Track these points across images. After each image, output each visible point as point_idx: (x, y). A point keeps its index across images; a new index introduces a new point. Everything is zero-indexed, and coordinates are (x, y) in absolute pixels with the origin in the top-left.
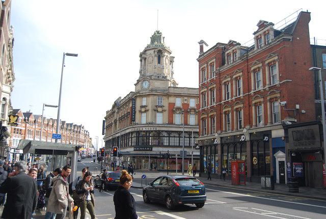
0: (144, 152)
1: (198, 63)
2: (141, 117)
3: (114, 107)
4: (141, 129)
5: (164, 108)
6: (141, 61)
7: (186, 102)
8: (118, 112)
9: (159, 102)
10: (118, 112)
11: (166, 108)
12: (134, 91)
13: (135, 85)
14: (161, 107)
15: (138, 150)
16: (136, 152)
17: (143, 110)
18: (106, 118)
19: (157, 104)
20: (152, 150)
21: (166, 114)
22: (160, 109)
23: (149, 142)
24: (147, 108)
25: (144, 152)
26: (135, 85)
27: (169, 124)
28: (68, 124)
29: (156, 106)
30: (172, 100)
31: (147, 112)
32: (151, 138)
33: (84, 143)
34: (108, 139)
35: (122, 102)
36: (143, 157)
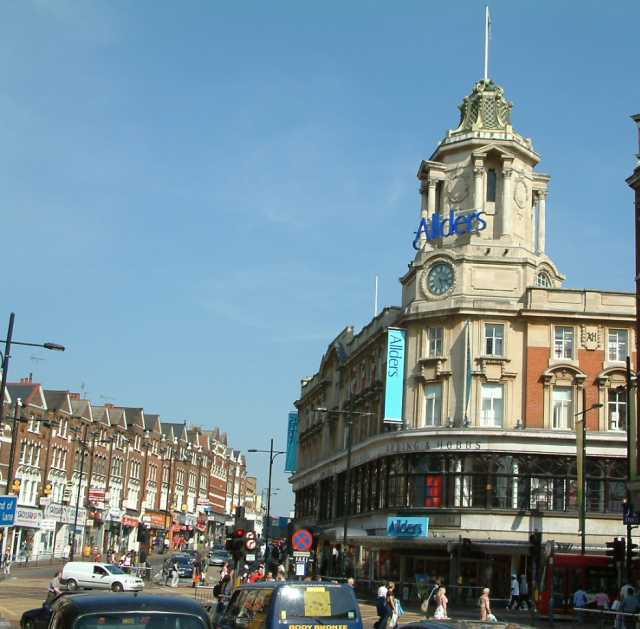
1: (633, 192)
3: (327, 364)
5: (508, 368)
7: (591, 345)
8: (341, 385)
9: (489, 342)
10: (341, 385)
11: (516, 366)
12: (399, 304)
14: (499, 362)
17: (428, 374)
18: (298, 405)
19: (483, 353)
21: (515, 389)
22: (492, 372)
27: (524, 425)
28: (166, 427)
29: (479, 361)
30: (539, 336)
32: (458, 482)
33: (224, 494)
34: (305, 483)
35: (355, 346)
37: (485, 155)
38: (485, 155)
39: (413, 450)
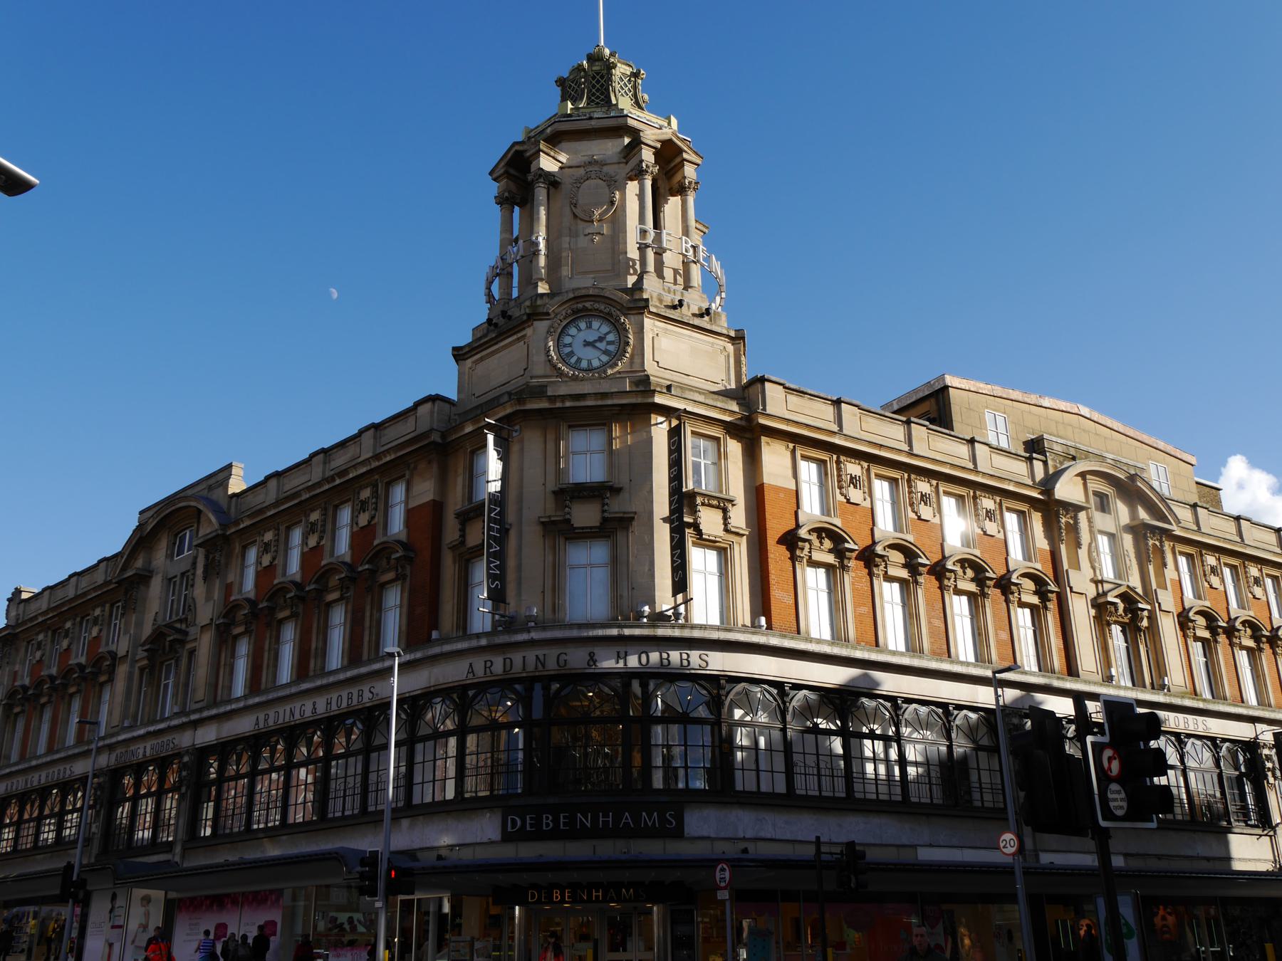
0: (608, 849)
2: (555, 586)
3: (142, 540)
4: (576, 659)
6: (506, 201)
12: (453, 396)
13: (460, 354)
15: (555, 835)
16: (529, 851)
17: (585, 515)
20: (678, 833)
23: (647, 767)
24: (617, 506)
25: (608, 849)
26: (460, 354)
31: (620, 536)
36: (656, 892)
37: (658, 145)
38: (658, 145)
39: (552, 665)
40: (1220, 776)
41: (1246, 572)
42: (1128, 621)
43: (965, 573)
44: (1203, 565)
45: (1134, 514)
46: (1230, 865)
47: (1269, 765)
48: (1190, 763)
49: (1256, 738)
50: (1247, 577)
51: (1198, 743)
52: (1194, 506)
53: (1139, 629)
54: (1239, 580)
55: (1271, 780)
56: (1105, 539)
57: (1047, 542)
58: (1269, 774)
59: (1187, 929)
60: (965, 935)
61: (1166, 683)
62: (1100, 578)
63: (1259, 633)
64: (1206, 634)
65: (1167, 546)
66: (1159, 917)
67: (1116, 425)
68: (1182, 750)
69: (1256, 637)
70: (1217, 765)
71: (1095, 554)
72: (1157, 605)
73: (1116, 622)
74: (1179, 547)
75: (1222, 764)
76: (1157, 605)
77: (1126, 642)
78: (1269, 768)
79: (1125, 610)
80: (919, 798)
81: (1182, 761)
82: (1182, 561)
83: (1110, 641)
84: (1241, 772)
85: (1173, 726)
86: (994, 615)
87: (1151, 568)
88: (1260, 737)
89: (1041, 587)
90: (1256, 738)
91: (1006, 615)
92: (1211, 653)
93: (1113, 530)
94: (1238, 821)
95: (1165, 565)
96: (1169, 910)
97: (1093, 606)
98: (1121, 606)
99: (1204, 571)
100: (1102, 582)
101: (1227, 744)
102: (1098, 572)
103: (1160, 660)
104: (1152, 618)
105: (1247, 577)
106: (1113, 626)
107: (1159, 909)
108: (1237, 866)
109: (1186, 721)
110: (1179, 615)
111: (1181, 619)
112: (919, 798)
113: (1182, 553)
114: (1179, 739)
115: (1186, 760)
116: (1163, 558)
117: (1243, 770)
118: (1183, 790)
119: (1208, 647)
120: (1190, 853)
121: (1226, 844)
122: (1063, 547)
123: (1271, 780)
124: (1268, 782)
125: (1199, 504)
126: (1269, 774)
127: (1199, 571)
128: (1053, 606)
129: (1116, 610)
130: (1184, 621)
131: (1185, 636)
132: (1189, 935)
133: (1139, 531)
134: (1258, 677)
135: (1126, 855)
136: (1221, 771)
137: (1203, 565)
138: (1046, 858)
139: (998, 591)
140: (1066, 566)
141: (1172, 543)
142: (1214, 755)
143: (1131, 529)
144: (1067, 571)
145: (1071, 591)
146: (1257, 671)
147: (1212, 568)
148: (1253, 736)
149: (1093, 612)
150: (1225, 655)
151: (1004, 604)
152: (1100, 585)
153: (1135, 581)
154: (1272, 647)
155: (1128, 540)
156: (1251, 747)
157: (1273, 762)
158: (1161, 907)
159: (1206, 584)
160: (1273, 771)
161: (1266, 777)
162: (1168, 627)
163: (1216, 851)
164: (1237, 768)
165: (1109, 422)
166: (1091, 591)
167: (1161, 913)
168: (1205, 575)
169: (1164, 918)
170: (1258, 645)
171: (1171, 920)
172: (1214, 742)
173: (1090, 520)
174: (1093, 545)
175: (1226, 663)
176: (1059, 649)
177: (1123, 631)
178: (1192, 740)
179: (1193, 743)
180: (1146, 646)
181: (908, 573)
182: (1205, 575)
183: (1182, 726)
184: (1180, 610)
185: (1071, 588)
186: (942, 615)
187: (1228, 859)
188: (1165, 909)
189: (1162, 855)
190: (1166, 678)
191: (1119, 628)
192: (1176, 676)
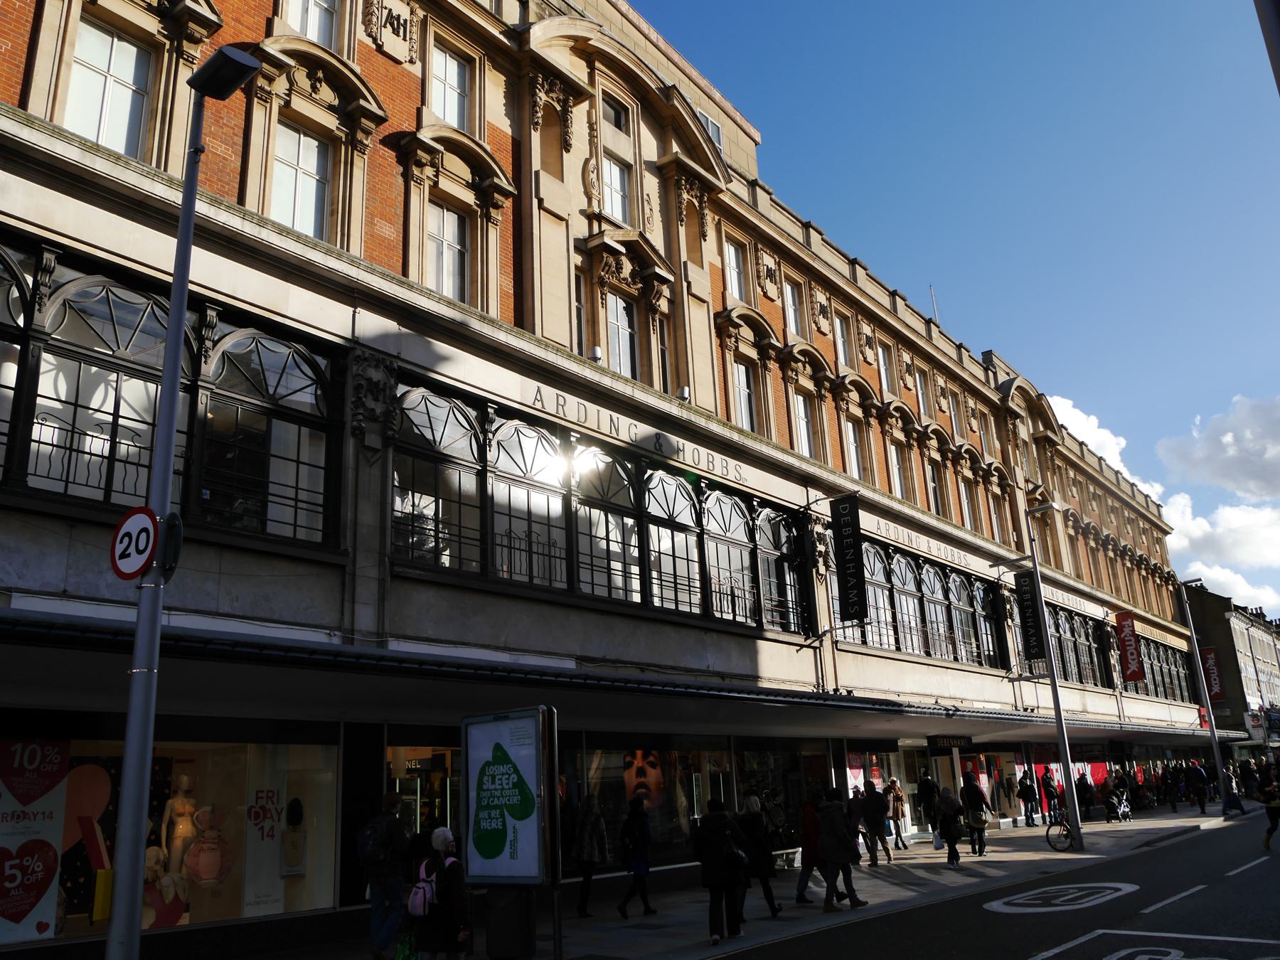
40: (753, 554)
41: (811, 296)
42: (636, 293)
43: (314, 89)
44: (757, 264)
45: (663, 147)
46: (757, 684)
47: (821, 548)
48: (711, 526)
49: (808, 507)
50: (812, 302)
51: (727, 501)
52: (753, 184)
53: (654, 310)
54: (801, 303)
55: (822, 569)
56: (616, 170)
57: (508, 122)
58: (821, 560)
59: (679, 786)
60: (181, 815)
61: (686, 395)
62: (597, 210)
63: (821, 374)
64: (753, 353)
65: (710, 218)
66: (633, 770)
67: (654, 35)
68: (700, 505)
69: (817, 378)
70: (752, 537)
71: (593, 176)
72: (685, 284)
73: (617, 291)
74: (726, 227)
75: (757, 537)
76: (685, 284)
77: (631, 325)
78: (820, 552)
79: (633, 274)
80: (67, 482)
81: (699, 522)
82: (730, 251)
83: (601, 311)
84: (782, 553)
85: (689, 461)
86: (372, 189)
87: (682, 230)
88: (813, 507)
89: (482, 179)
90: (808, 507)
91: (401, 199)
92: (757, 383)
93: (630, 159)
94: (773, 623)
95: (703, 236)
96: (652, 759)
97: (578, 249)
98: (627, 267)
99: (758, 272)
100: (600, 218)
101: (767, 511)
102: (595, 203)
103: (682, 366)
104: (675, 302)
105: (812, 302)
106: (611, 298)
107: (634, 757)
108: (764, 684)
109: (711, 460)
110: (717, 315)
111: (719, 321)
112: (67, 482)
113: (731, 239)
114: (699, 486)
115: (705, 521)
116: (702, 225)
117: (784, 550)
118: (696, 567)
119: (754, 371)
120: (694, 664)
121: (753, 656)
122: (536, 137)
123: (822, 569)
124: (817, 571)
125: (760, 182)
126: (821, 560)
127: (751, 269)
128: (503, 215)
129: (619, 267)
130: (723, 324)
131: (723, 346)
132: (683, 801)
133: (668, 173)
134: (815, 433)
135: (580, 659)
136: (756, 546)
137: (757, 264)
138: (396, 646)
139: (390, 155)
140: (536, 164)
141: (717, 218)
142: (747, 523)
143: (658, 169)
144: (537, 173)
145: (541, 206)
146: (814, 426)
147: (769, 270)
148: (804, 503)
149: (577, 259)
150: (776, 391)
151: (400, 180)
152: (596, 225)
153: (657, 238)
154: (834, 400)
155: (651, 184)
156: (798, 518)
157: (826, 545)
158: (639, 753)
159: (759, 290)
160: (825, 555)
161: (815, 564)
162: (698, 323)
163: (735, 665)
164: (777, 546)
165: (644, 26)
166: (580, 228)
167: (638, 762)
168: (759, 277)
169: (641, 772)
170: (819, 391)
171: (653, 775)
172: (748, 501)
173: (592, 127)
174: (593, 161)
175: (776, 402)
176: (503, 294)
177: (628, 310)
178: (717, 493)
179: (718, 500)
180: (663, 343)
181: (160, 22)
182: (759, 277)
183: (703, 466)
184: (720, 309)
185: (541, 201)
186: (240, 141)
187: (756, 678)
188: (645, 757)
189: (649, 665)
190: (687, 389)
191: (621, 304)
192: (703, 390)
